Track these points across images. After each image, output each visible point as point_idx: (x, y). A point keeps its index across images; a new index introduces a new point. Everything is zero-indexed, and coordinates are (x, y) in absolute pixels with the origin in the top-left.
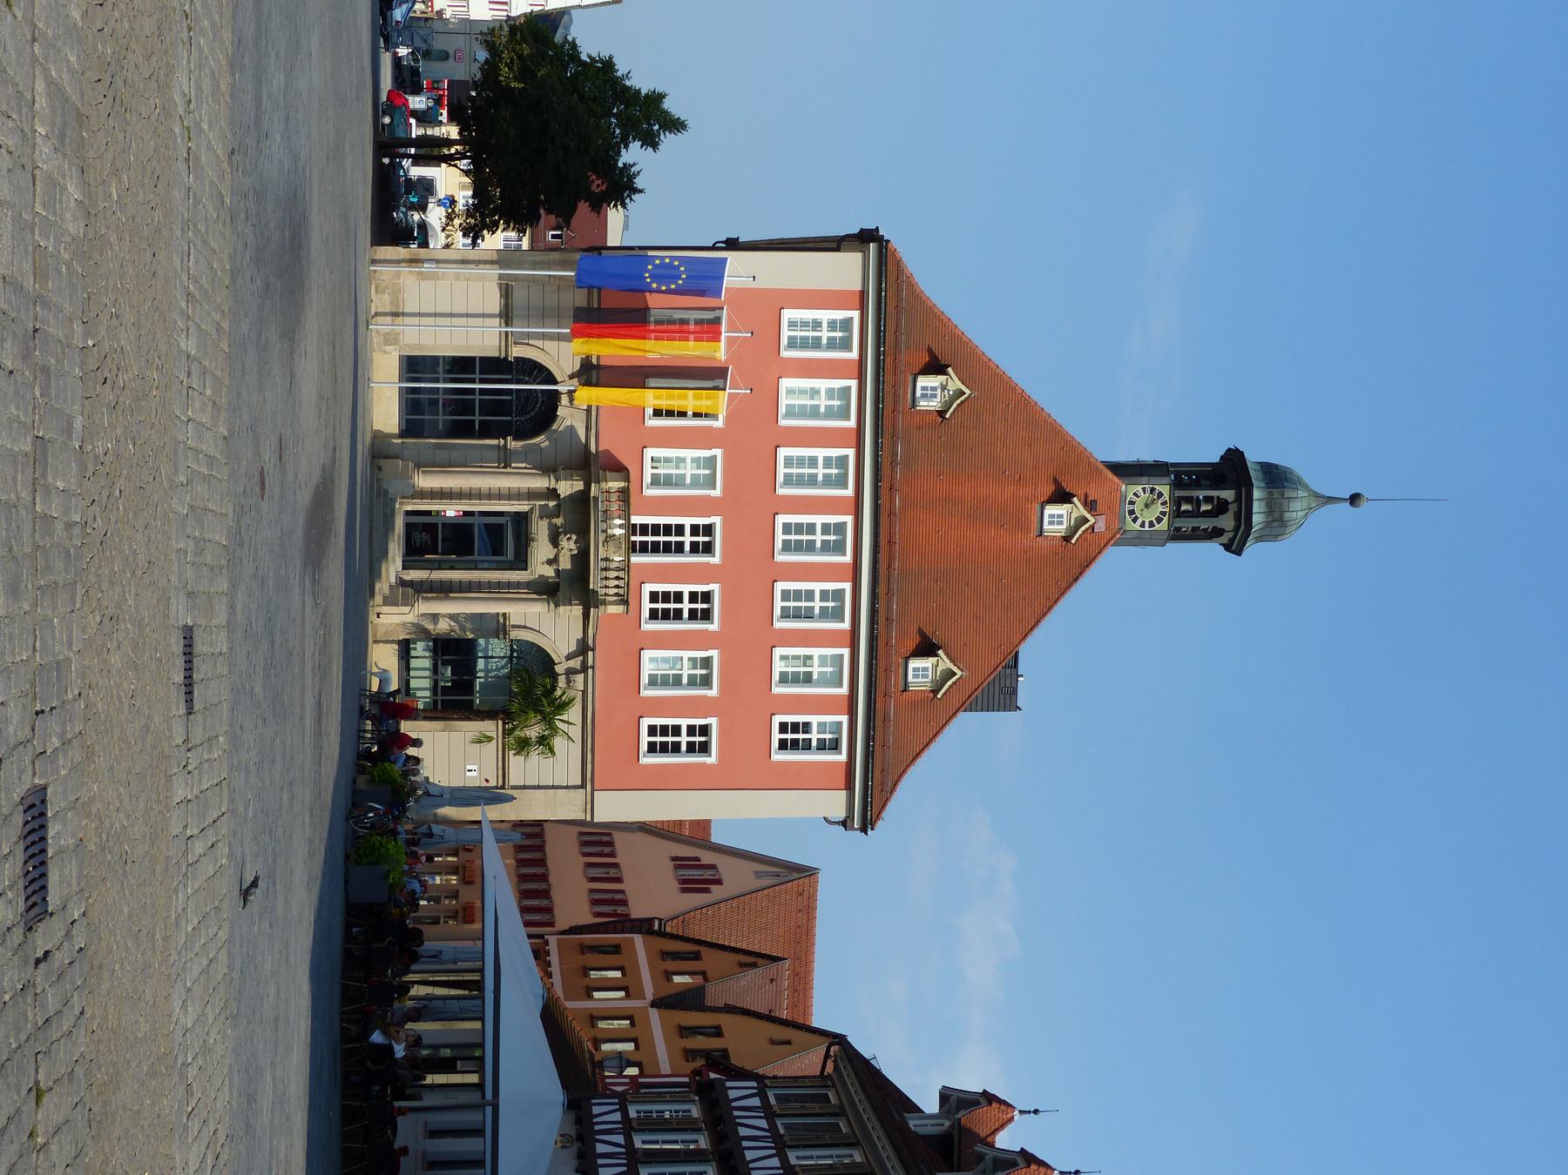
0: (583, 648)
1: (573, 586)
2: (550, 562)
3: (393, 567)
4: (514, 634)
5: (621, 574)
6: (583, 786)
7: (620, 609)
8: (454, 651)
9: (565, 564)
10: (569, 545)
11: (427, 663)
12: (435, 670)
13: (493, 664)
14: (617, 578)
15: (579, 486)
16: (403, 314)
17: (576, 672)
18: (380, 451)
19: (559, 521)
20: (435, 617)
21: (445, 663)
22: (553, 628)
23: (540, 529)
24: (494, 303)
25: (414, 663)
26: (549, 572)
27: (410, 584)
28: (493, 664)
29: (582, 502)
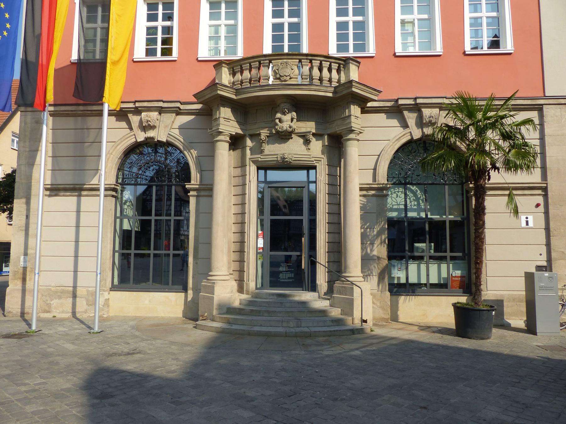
0: (396, 111)
1: (330, 112)
2: (307, 142)
3: (314, 300)
4: (382, 178)
5: (316, 63)
6: (539, 109)
7: (353, 67)
8: (403, 239)
9: (310, 126)
10: (287, 120)
11: (413, 267)
12: (421, 258)
13: (412, 204)
14: (320, 69)
15: (225, 112)
16: (75, 287)
17: (420, 117)
18: (192, 314)
19: (264, 133)
20: (366, 260)
21: (412, 249)
22: (374, 142)
23: (274, 151)
24: (68, 202)
25: (413, 279)
26: (317, 146)
27: (331, 283)
28: (412, 204)
29: (245, 109)
